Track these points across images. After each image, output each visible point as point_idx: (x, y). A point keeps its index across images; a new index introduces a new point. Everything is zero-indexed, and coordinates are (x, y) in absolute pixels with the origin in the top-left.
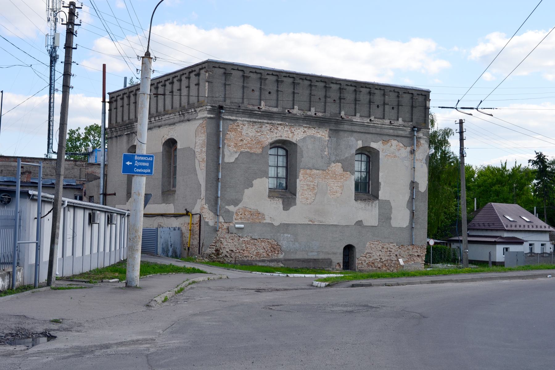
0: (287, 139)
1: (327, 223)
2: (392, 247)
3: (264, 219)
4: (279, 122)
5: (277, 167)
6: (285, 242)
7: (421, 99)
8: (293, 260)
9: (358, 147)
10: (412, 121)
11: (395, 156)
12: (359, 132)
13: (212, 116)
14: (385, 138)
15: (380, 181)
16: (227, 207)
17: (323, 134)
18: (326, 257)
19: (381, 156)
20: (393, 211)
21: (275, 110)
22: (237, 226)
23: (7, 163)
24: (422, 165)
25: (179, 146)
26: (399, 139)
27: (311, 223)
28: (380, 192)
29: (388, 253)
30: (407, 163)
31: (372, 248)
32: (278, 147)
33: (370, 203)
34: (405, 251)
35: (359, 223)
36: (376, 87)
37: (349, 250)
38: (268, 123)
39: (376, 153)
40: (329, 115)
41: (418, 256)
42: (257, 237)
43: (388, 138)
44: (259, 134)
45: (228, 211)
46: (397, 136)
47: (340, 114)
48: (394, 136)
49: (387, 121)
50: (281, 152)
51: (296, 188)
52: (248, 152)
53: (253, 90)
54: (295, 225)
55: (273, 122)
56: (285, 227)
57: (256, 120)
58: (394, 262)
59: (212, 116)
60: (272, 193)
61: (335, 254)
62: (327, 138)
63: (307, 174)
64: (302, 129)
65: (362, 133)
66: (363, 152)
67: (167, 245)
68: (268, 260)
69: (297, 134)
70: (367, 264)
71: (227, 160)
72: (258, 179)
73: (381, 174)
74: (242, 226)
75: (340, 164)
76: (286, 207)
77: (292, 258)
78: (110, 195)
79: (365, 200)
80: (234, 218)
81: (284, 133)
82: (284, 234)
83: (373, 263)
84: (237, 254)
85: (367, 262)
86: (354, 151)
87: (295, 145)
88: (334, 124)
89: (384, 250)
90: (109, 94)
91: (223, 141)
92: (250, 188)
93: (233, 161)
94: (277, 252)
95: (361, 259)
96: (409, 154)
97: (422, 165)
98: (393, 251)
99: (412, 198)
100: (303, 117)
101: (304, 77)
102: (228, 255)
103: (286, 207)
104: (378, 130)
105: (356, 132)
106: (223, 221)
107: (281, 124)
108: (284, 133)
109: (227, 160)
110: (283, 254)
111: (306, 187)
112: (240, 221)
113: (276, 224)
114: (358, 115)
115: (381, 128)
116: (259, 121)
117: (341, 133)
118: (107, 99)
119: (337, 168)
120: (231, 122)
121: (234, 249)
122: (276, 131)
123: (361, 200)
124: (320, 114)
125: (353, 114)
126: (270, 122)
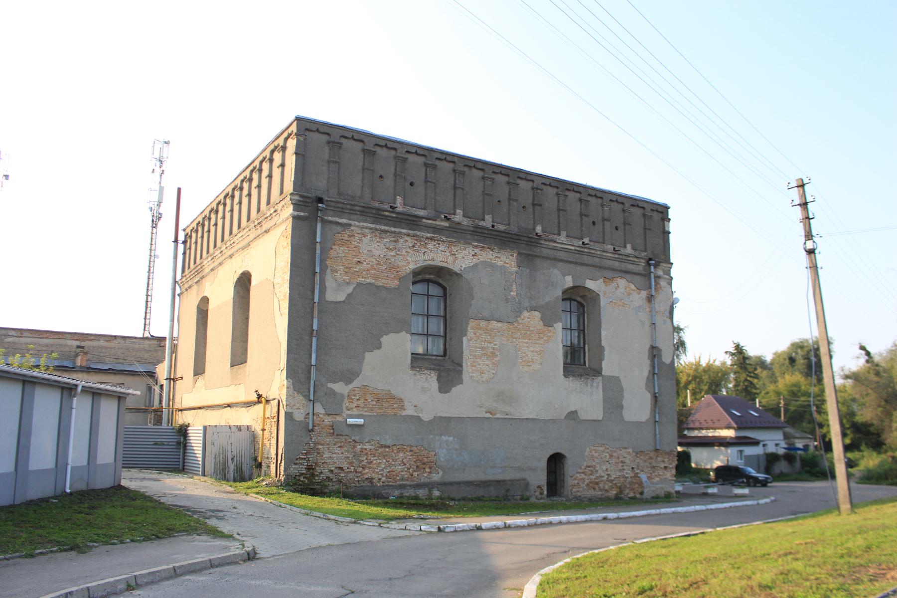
0: (444, 265)
1: (517, 416)
3: (402, 408)
4: (429, 235)
5: (428, 316)
6: (444, 450)
7: (656, 217)
8: (459, 483)
9: (566, 286)
10: (645, 251)
11: (624, 305)
12: (567, 262)
13: (302, 214)
15: (603, 343)
16: (330, 385)
17: (507, 260)
18: (517, 475)
19: (602, 303)
20: (626, 395)
22: (350, 421)
23: (61, 342)
24: (665, 321)
25: (253, 282)
26: (628, 276)
27: (488, 415)
28: (604, 364)
29: (620, 464)
30: (644, 316)
31: (593, 458)
32: (428, 281)
33: (589, 381)
35: (572, 415)
36: (590, 192)
37: (556, 461)
38: (408, 235)
39: (594, 298)
40: (516, 230)
41: (666, 468)
42: (389, 443)
43: (610, 274)
44: (393, 253)
45: (333, 393)
46: (627, 272)
47: (534, 229)
48: (621, 271)
49: (610, 248)
50: (434, 290)
51: (462, 353)
52: (369, 284)
53: (381, 177)
54: (460, 419)
55: (418, 233)
56: (444, 424)
57: (386, 228)
58: (629, 480)
59: (302, 214)
60: (418, 361)
61: (533, 470)
62: (515, 269)
63: (480, 328)
64: (470, 250)
65: (571, 262)
66: (573, 297)
67: (226, 458)
68: (410, 486)
69: (461, 258)
70: (588, 485)
71: (330, 296)
72: (392, 335)
73: (603, 333)
74: (361, 421)
75: (537, 314)
76: (445, 385)
77: (457, 480)
79: (581, 376)
80: (344, 406)
81: (438, 254)
83: (597, 483)
84: (351, 476)
85: (587, 481)
86: (559, 293)
87: (458, 275)
89: (614, 460)
91: (322, 261)
92: (376, 352)
93: (343, 299)
94: (427, 470)
95: (575, 479)
96: (645, 301)
97: (665, 321)
98: (627, 461)
99: (653, 373)
100: (472, 229)
101: (472, 164)
102: (331, 476)
103: (445, 385)
104: (597, 260)
105: (562, 261)
106: (323, 411)
108: (438, 254)
109: (330, 296)
110: (441, 473)
111: (479, 352)
112: (356, 412)
113: (426, 417)
114: (564, 233)
115: (601, 257)
116: (393, 229)
117: (538, 261)
118: (181, 237)
119: (533, 319)
120: (339, 229)
121: (345, 466)
122: (423, 250)
123: (574, 376)
124: (501, 227)
125: (556, 232)
126: (411, 232)
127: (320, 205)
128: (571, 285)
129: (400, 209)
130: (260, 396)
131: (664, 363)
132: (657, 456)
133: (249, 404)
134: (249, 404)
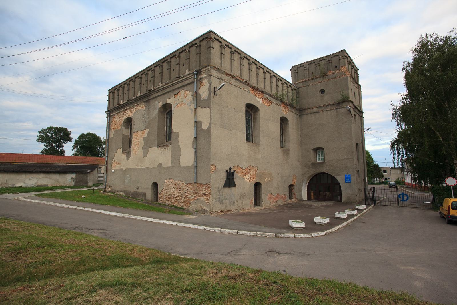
0: (129, 116)
2: (181, 185)
14: (176, 92)
17: (142, 107)
21: (126, 102)
26: (185, 88)
34: (191, 189)
35: (160, 165)
41: (205, 194)
58: (183, 198)
70: (165, 198)
83: (169, 198)
86: (157, 111)
88: (146, 98)
89: (176, 188)
93: (112, 137)
107: (126, 110)
117: (151, 101)
128: (161, 105)
129: (122, 104)
131: (204, 130)
132: (198, 187)
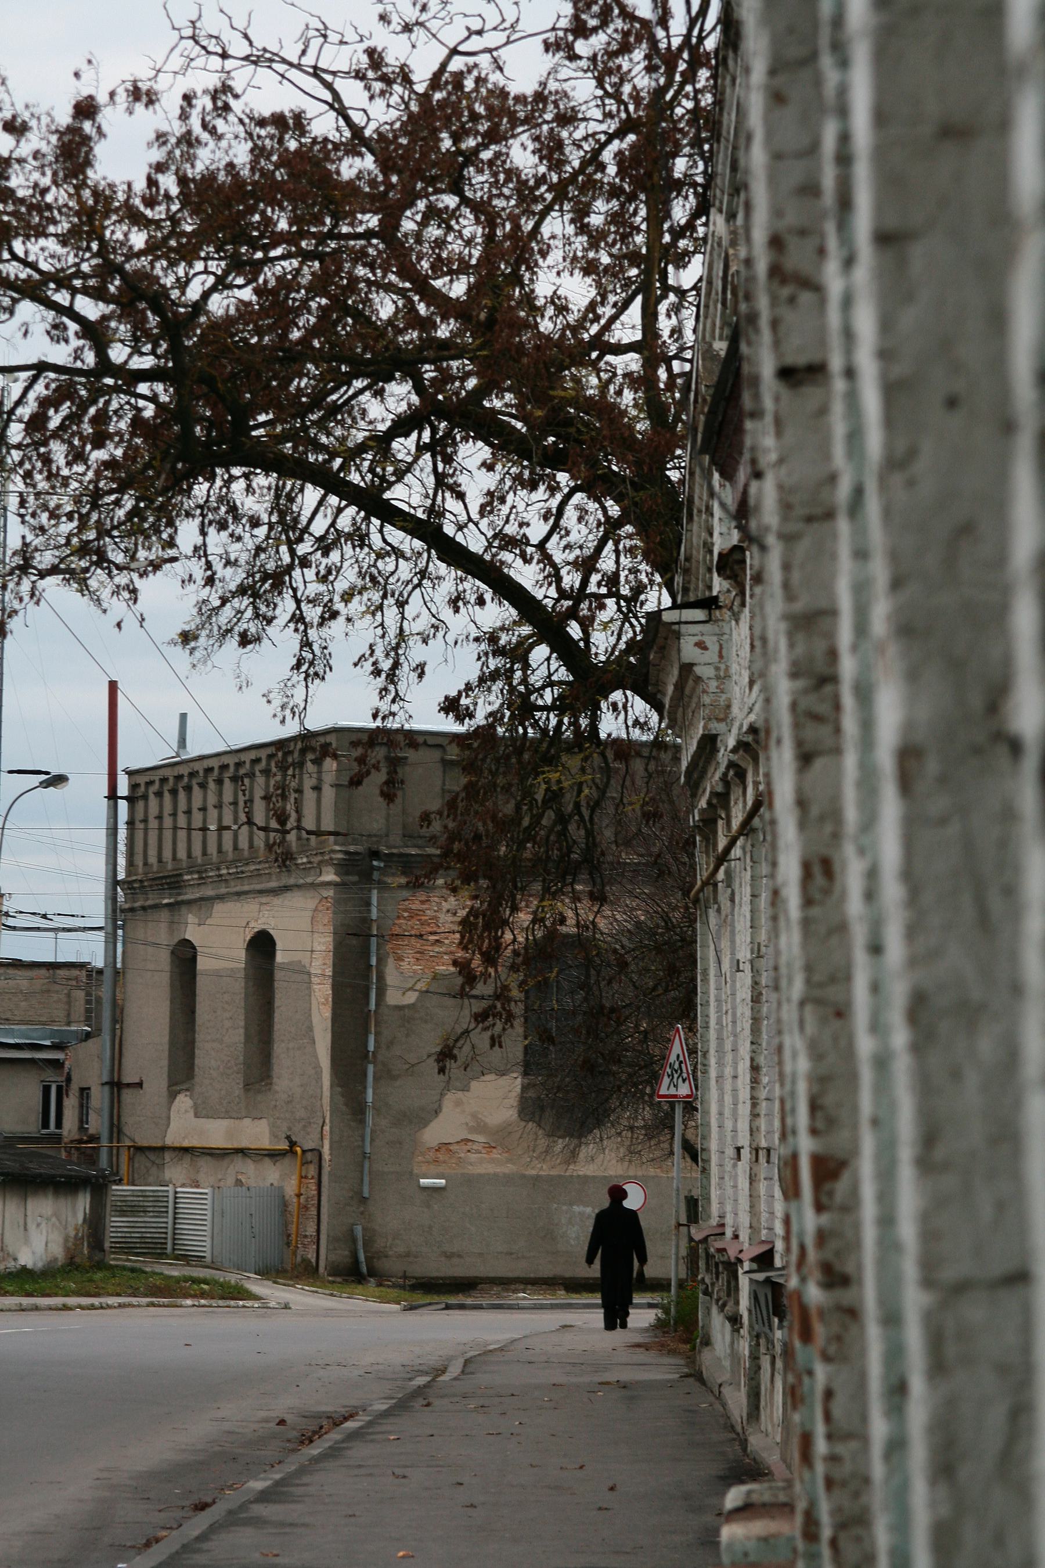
22: (423, 1182)
71: (393, 998)
78: (129, 1085)
82: (571, 1204)
90: (130, 773)
118: (123, 789)
127: (375, 863)
130: (293, 1144)
133: (274, 1155)
134: (274, 1155)
